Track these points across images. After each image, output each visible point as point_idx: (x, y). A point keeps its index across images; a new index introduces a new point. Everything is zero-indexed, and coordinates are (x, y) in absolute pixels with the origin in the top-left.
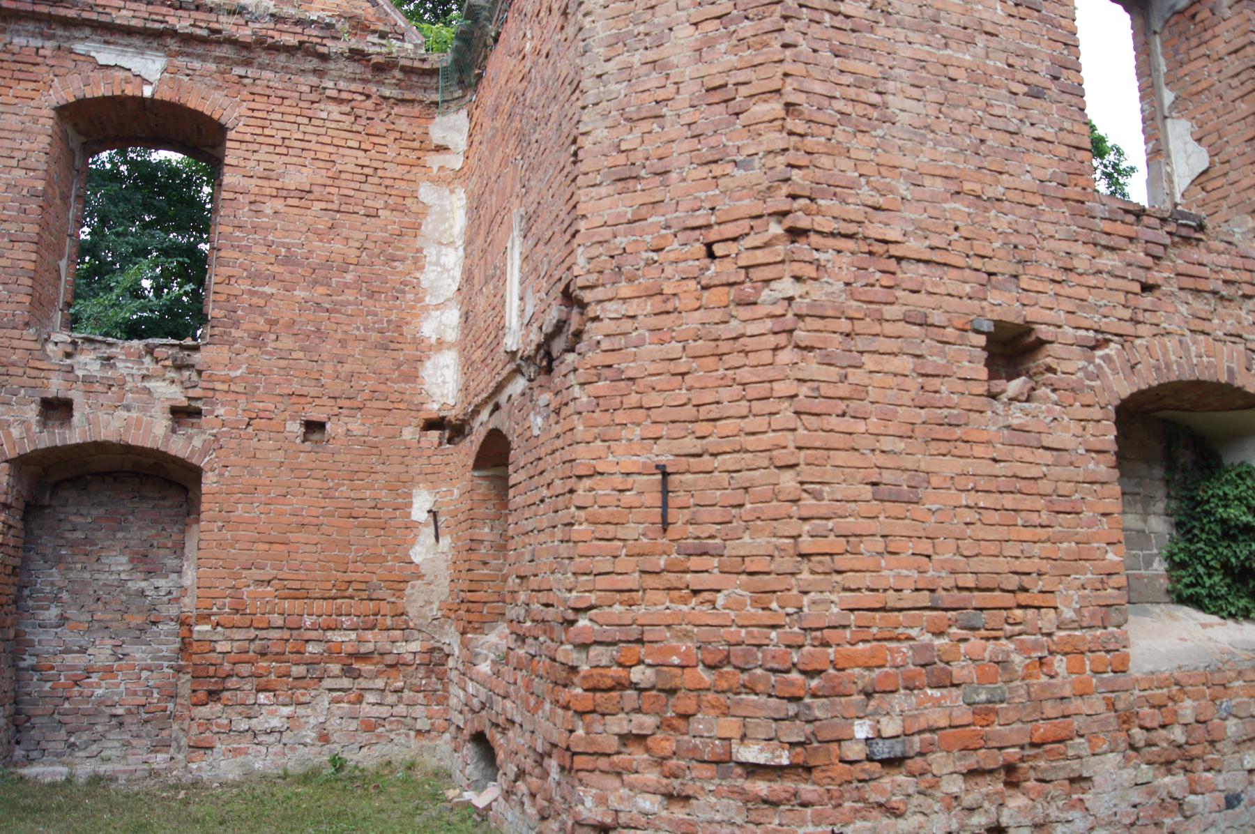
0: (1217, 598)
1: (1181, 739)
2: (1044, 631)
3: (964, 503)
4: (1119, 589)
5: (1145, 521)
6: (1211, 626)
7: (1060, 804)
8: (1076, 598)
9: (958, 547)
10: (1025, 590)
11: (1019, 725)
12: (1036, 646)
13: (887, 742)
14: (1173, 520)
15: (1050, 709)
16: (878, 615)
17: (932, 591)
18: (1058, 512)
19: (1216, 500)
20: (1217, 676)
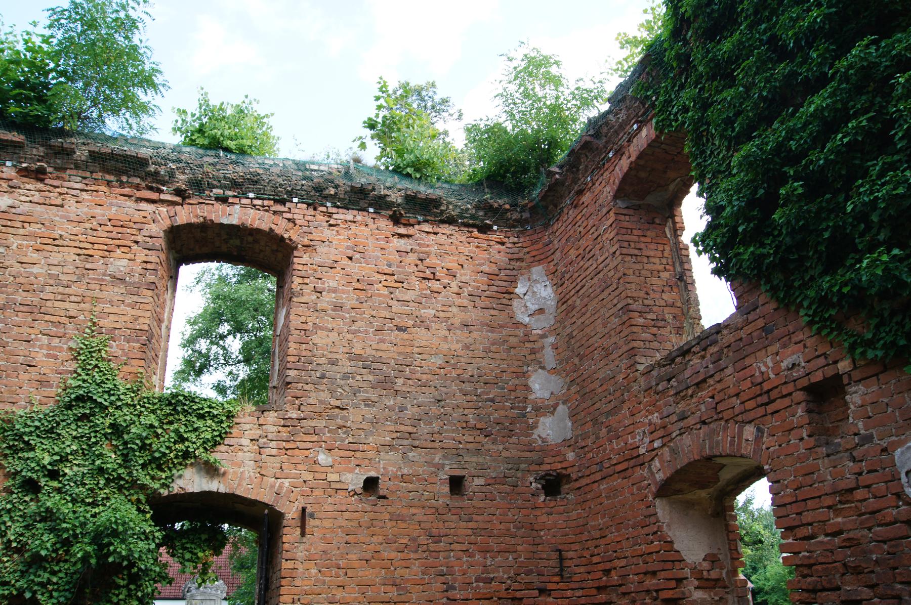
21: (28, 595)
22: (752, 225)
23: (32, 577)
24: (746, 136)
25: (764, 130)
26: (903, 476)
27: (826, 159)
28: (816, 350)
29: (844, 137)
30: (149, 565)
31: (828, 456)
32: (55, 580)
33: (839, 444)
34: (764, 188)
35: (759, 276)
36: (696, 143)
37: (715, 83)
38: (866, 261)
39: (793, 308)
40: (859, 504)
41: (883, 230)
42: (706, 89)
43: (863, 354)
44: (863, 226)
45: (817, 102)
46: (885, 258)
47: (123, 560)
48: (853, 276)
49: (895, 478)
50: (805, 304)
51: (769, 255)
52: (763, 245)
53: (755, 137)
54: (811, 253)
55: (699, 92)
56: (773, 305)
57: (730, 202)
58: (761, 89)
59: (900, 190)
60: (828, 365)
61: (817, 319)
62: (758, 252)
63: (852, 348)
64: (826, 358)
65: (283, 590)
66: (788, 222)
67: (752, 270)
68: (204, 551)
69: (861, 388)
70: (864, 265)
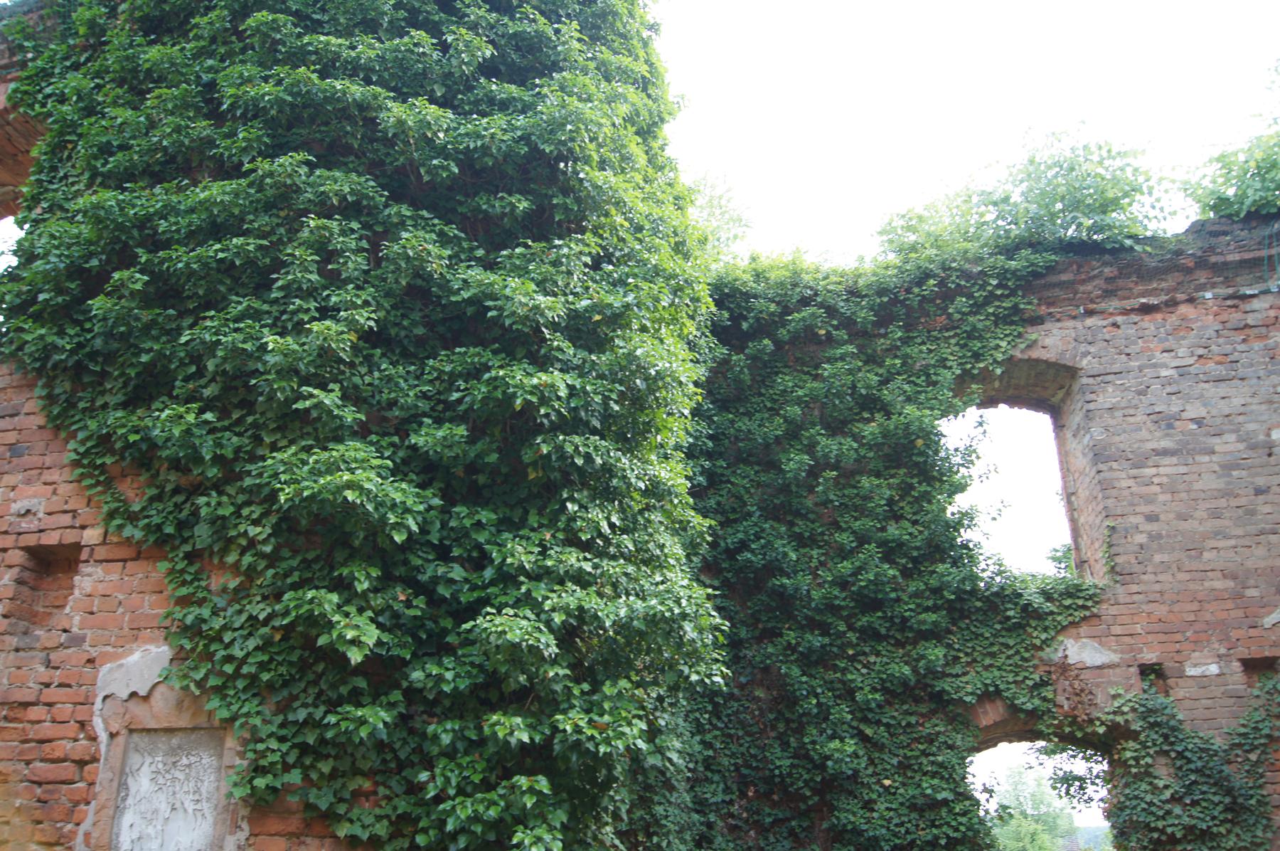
22: (60, 299)
24: (118, 180)
25: (143, 189)
26: (99, 700)
27: (187, 264)
28: (66, 502)
29: (222, 251)
31: (17, 650)
33: (38, 639)
34: (100, 260)
35: (40, 372)
36: (53, 152)
37: (120, 91)
38: (167, 412)
39: (63, 435)
40: (29, 726)
41: (213, 384)
42: (105, 90)
43: (120, 527)
44: (193, 369)
45: (215, 191)
46: (191, 418)
48: (150, 424)
49: (87, 702)
50: (81, 436)
51: (63, 349)
52: (61, 333)
53: (124, 190)
54: (116, 373)
55: (93, 89)
56: (40, 420)
57: (46, 254)
58: (163, 136)
59: (248, 346)
60: (72, 527)
61: (85, 462)
62: (49, 339)
63: (111, 515)
64: (74, 517)
66: (105, 319)
67: (36, 360)
69: (98, 571)
70: (163, 416)
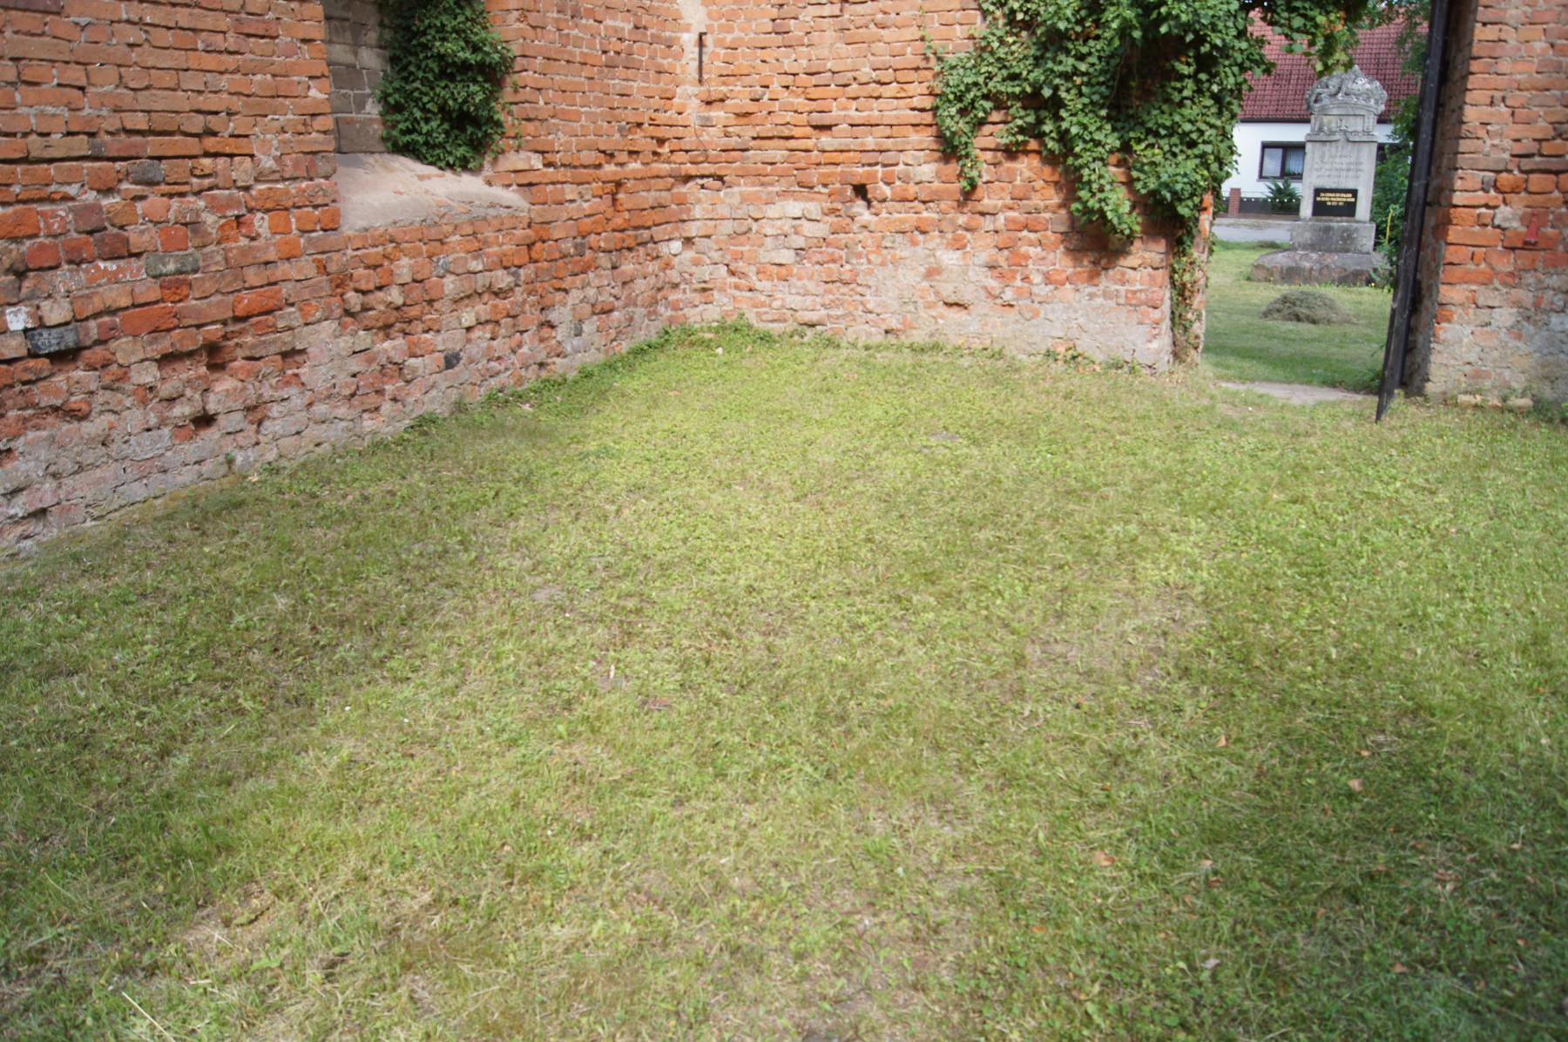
0: (434, 146)
1: (399, 301)
2: (240, 184)
3: (125, 17)
4: (325, 132)
5: (356, 54)
6: (429, 177)
7: (274, 381)
8: (275, 142)
9: (121, 77)
10: (215, 134)
11: (219, 297)
12: (231, 203)
13: (54, 331)
14: (387, 53)
15: (253, 276)
16: (19, 169)
17: (92, 135)
18: (249, 35)
19: (433, 32)
20: (433, 230)
21: (1047, 92)
23: (1050, 65)
30: (1228, 39)
32: (1083, 67)
47: (1186, 32)
65: (1472, 82)
68: (1328, 13)
